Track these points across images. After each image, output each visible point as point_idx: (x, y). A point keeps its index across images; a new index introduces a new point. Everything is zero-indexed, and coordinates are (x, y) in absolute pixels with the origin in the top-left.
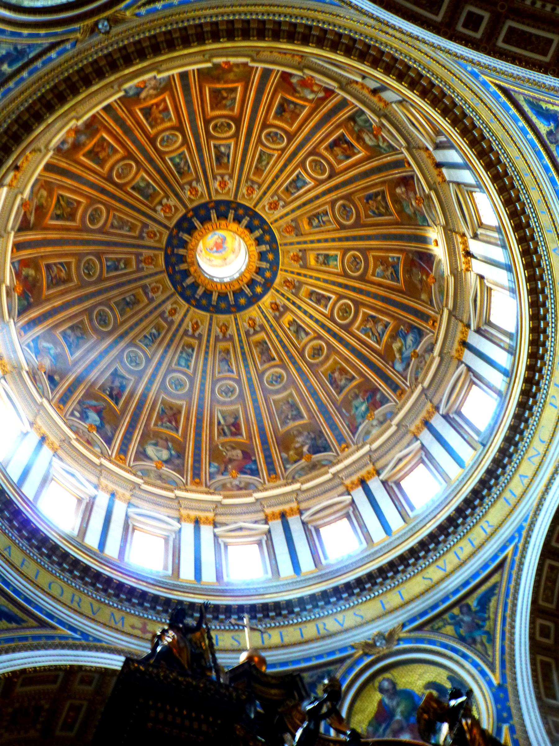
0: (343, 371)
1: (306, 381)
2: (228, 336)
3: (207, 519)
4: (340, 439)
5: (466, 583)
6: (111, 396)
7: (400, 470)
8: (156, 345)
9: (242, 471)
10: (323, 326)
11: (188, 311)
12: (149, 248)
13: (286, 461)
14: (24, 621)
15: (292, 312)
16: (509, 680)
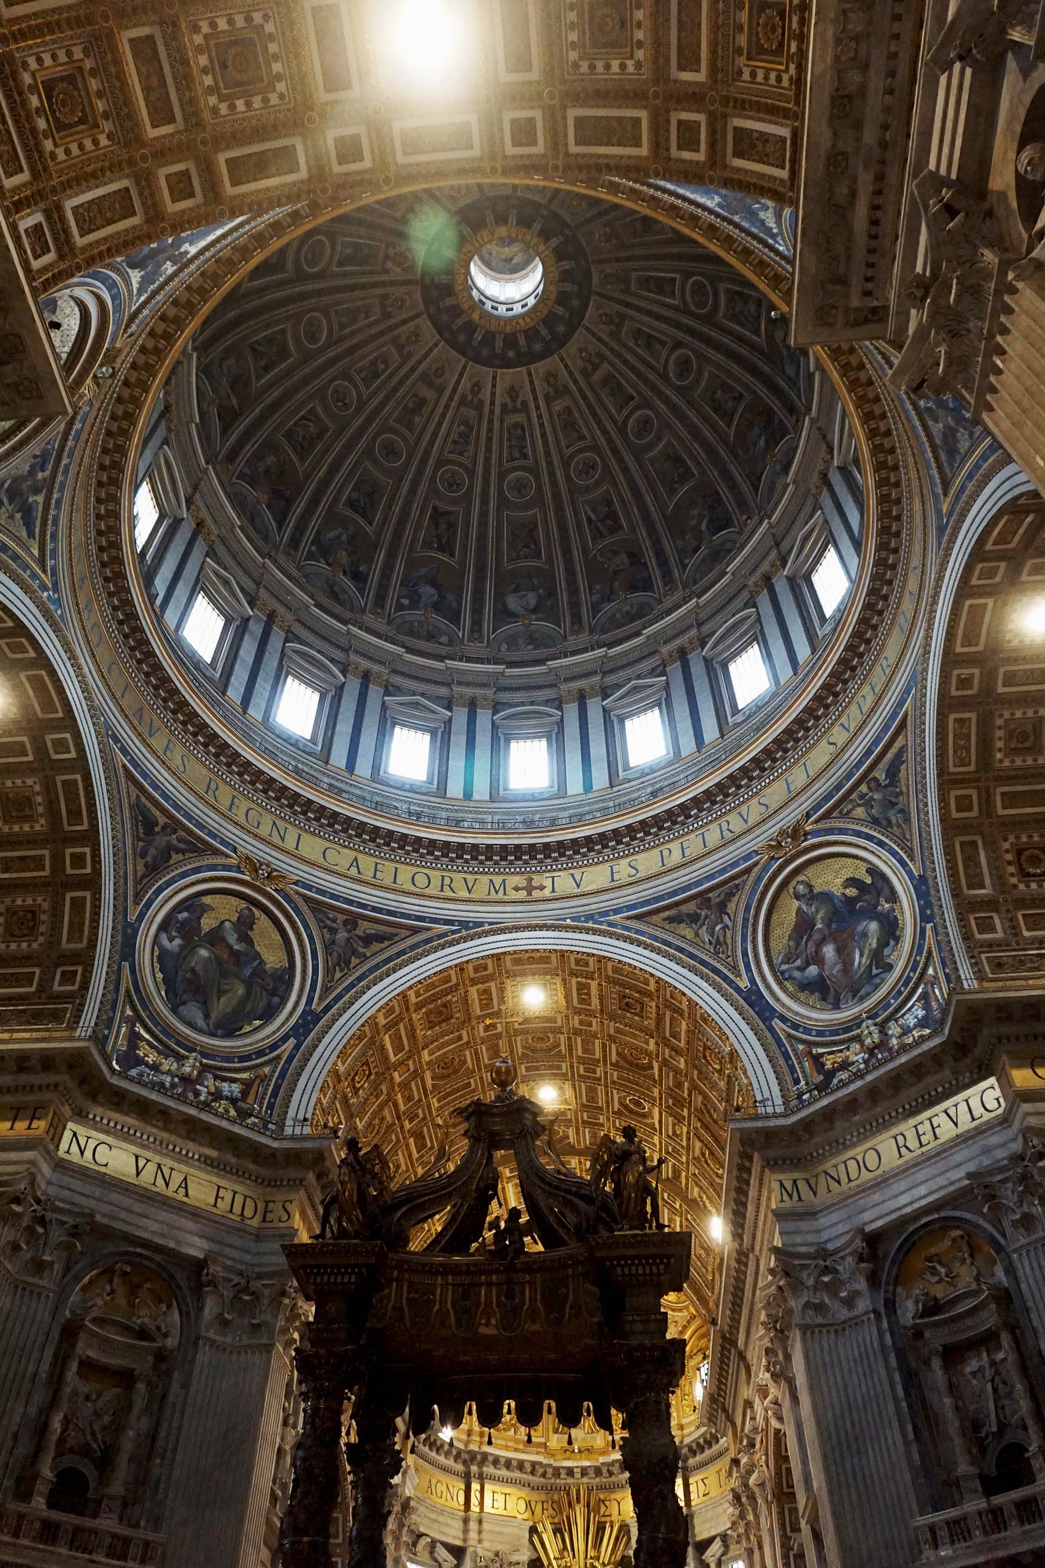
0: (726, 387)
1: (683, 417)
2: (561, 388)
3: (592, 688)
4: (742, 504)
5: (868, 753)
6: (441, 549)
7: (808, 556)
8: (472, 447)
9: (634, 588)
10: (678, 326)
11: (494, 378)
12: (404, 322)
13: (683, 554)
14: (396, 935)
15: (632, 318)
16: (929, 873)
